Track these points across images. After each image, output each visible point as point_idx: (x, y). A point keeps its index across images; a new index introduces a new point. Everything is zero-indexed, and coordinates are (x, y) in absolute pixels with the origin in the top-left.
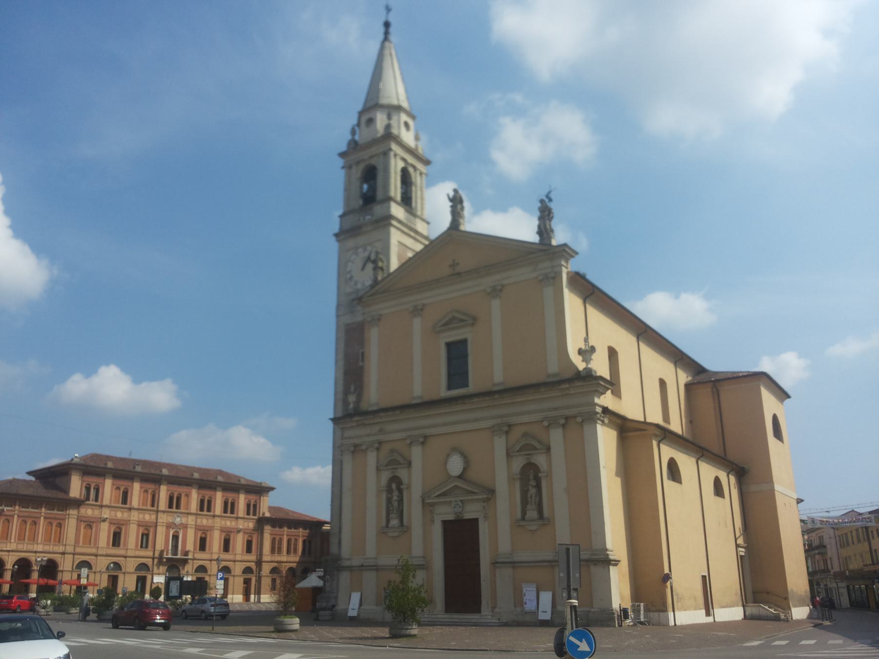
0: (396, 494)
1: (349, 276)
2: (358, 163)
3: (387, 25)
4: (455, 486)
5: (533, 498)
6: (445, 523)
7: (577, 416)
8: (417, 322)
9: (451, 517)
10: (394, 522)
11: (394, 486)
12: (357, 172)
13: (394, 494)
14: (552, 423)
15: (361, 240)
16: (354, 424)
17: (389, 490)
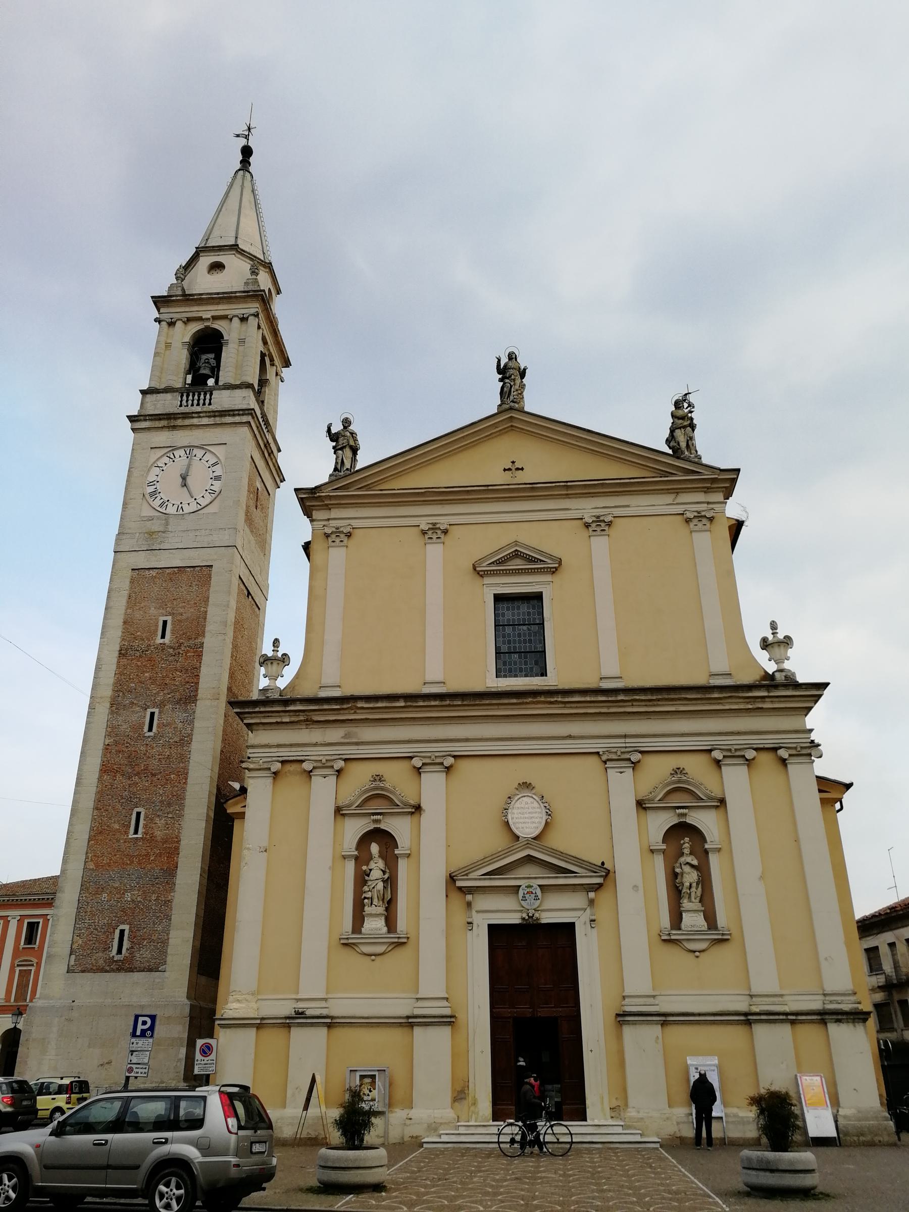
0: (377, 868)
1: (151, 489)
2: (189, 320)
3: (247, 152)
4: (529, 855)
5: (693, 889)
6: (494, 930)
7: (780, 748)
8: (435, 551)
9: (514, 919)
10: (375, 925)
11: (375, 848)
12: (185, 334)
13: (372, 865)
14: (735, 755)
15: (182, 437)
16: (287, 720)
17: (362, 858)
